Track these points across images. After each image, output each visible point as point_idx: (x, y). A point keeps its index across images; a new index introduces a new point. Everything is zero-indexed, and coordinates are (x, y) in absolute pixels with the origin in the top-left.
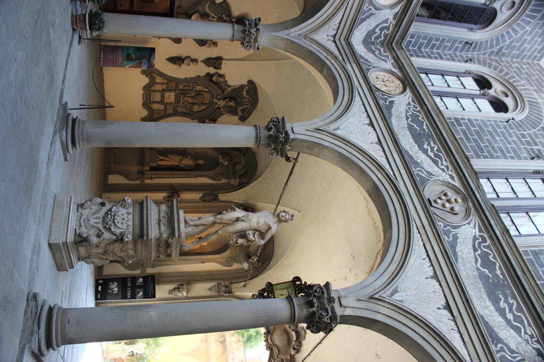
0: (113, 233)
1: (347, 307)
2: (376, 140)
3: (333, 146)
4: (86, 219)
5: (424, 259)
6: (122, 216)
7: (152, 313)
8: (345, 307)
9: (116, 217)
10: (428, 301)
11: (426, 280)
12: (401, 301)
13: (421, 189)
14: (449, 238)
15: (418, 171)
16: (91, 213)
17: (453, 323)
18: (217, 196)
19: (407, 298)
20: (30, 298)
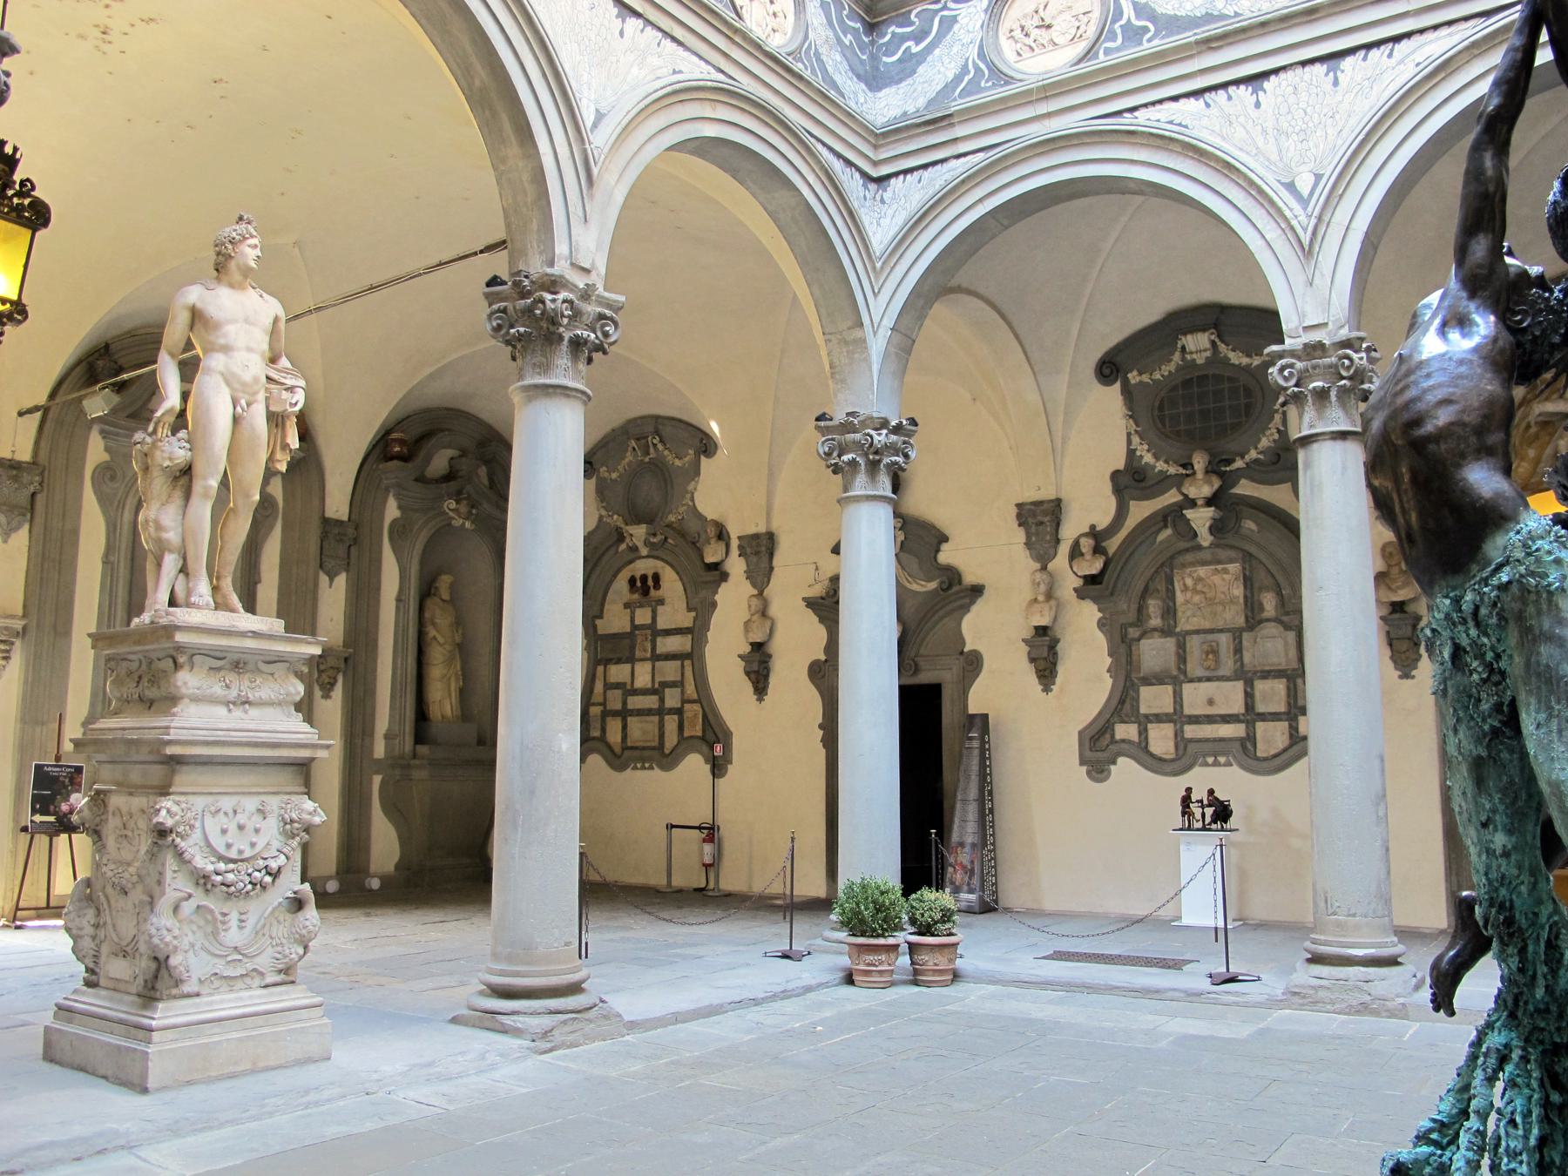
4: (229, 958)
6: (229, 834)
7: (564, 747)
9: (233, 854)
12: (600, 117)
16: (207, 944)
20: (549, 1045)
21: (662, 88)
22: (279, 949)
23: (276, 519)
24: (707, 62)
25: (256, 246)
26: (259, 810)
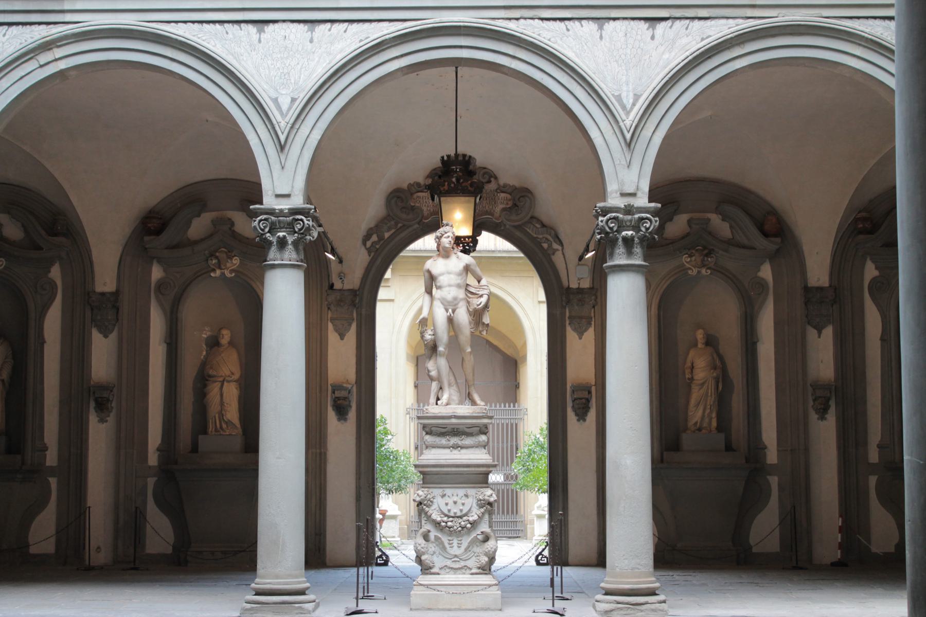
0: (480, 518)
1: (638, 186)
4: (453, 560)
5: (568, 30)
6: (449, 505)
7: (628, 462)
8: (638, 189)
9: (452, 514)
10: (639, 51)
11: (603, 40)
12: (637, 97)
18: (103, 294)
19: (631, 84)
21: (683, 61)
22: (478, 558)
23: (767, 294)
25: (449, 237)
26: (465, 495)
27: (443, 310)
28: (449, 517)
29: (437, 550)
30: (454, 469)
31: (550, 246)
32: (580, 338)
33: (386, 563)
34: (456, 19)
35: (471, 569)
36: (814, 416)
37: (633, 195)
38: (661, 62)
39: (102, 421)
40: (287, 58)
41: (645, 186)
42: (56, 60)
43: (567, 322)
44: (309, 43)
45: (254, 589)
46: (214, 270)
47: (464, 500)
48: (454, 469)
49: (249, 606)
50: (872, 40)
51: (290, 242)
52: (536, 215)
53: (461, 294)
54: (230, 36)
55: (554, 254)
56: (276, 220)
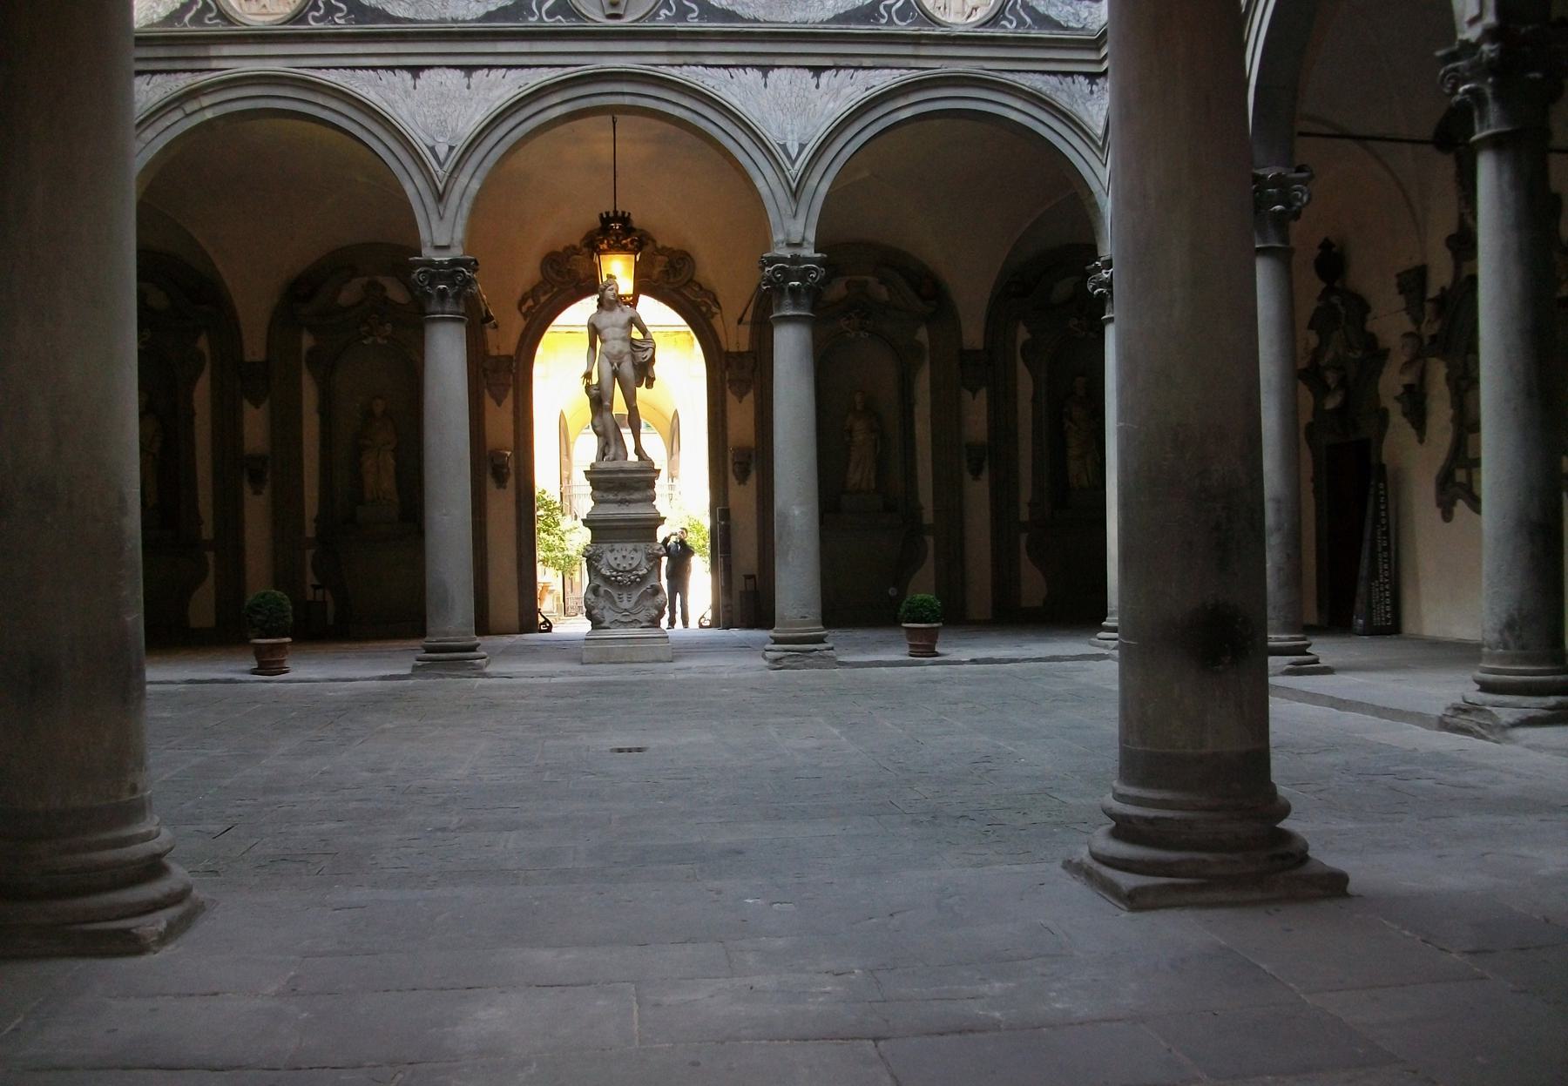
2: (459, 74)
3: (481, 174)
7: (797, 512)
8: (804, 239)
9: (621, 569)
10: (804, 100)
12: (802, 147)
13: (590, 25)
14: (693, 11)
15: (539, 9)
17: (842, 72)
20: (778, 666)
24: (898, 68)
27: (608, 364)
28: (618, 571)
29: (608, 605)
30: (622, 524)
31: (709, 308)
32: (740, 402)
33: (549, 630)
34: (617, 65)
35: (641, 623)
36: (968, 476)
37: (799, 245)
38: (826, 112)
39: (257, 492)
40: (444, 104)
41: (811, 236)
42: (203, 109)
43: (728, 385)
44: (466, 90)
45: (424, 647)
46: (365, 338)
47: (634, 554)
48: (622, 524)
49: (420, 663)
50: (1031, 93)
51: (450, 295)
52: (695, 278)
53: (626, 348)
54: (384, 82)
55: (713, 317)
56: (436, 272)
